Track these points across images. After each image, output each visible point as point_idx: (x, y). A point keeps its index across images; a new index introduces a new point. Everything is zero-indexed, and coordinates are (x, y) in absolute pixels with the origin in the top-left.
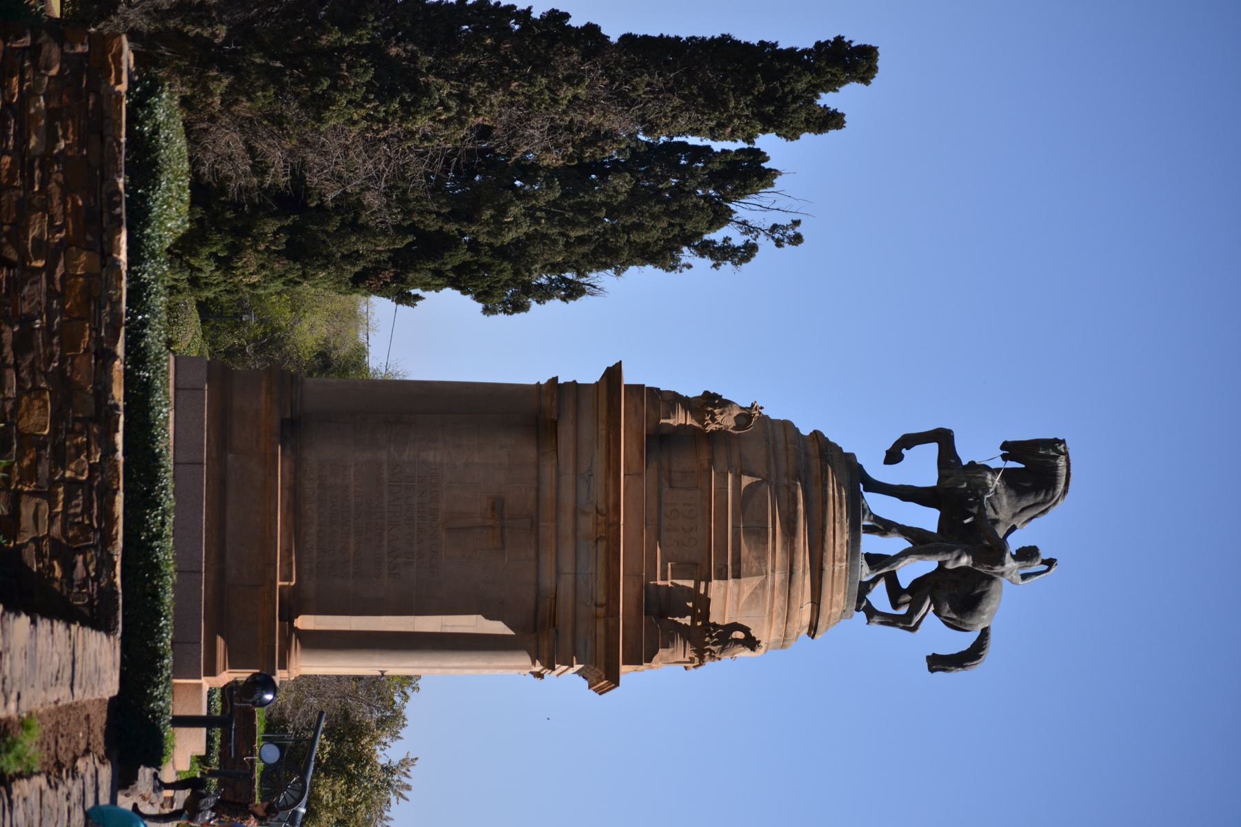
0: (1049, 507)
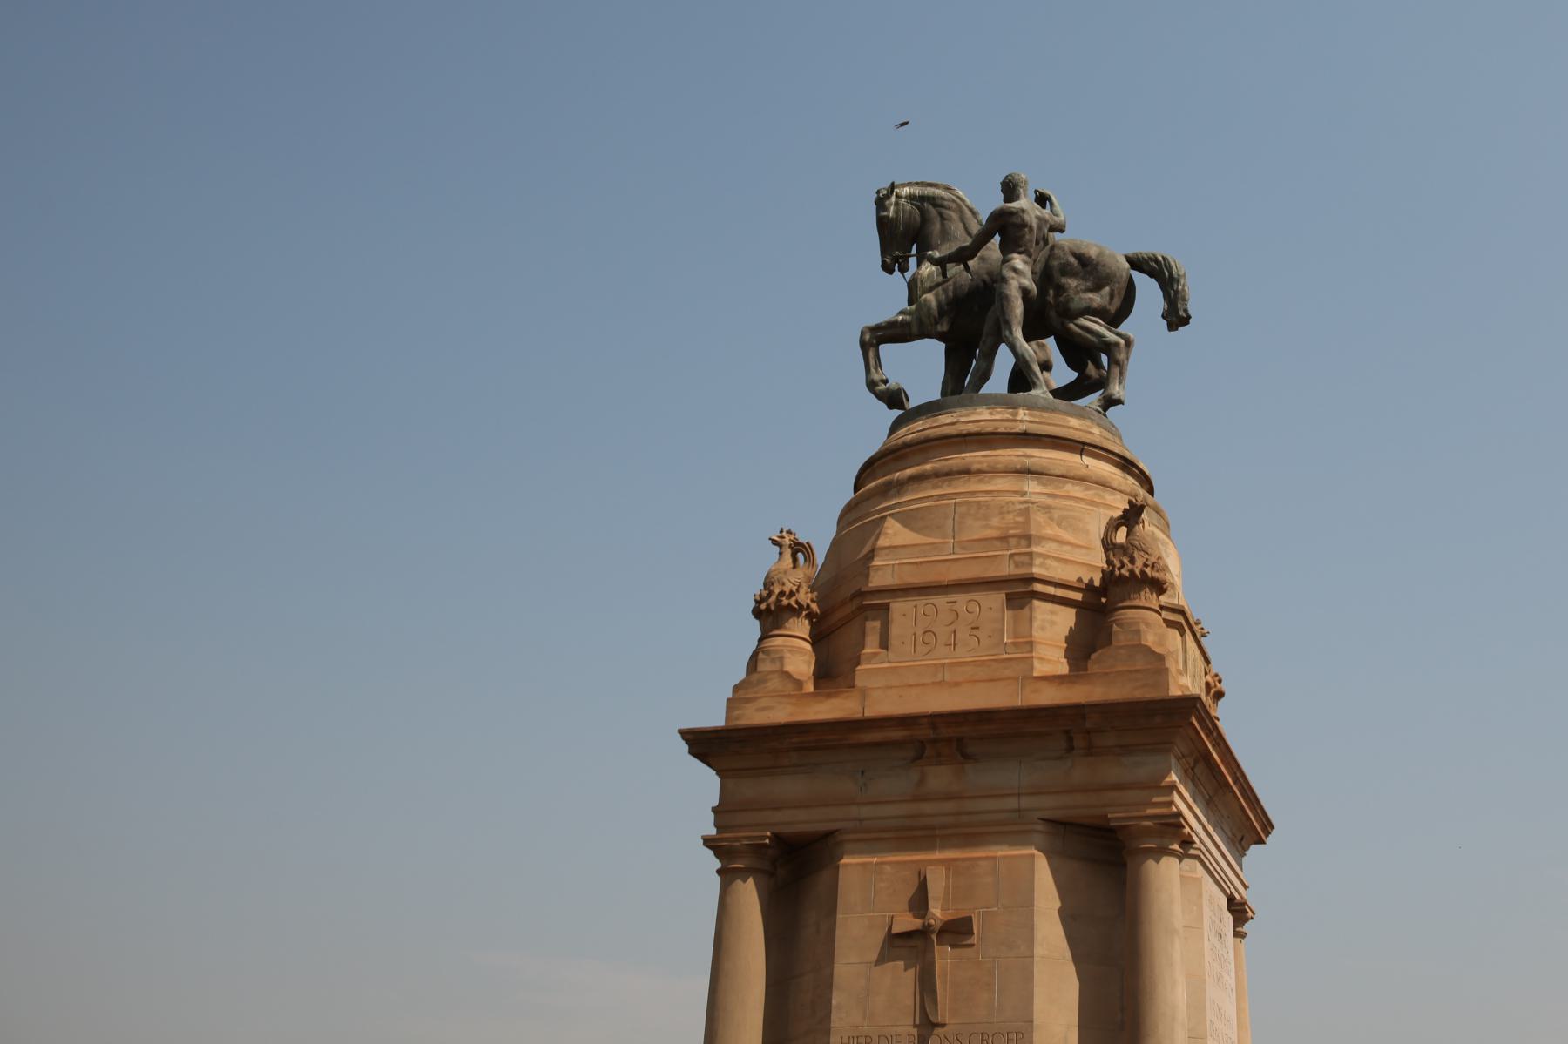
0: (967, 207)
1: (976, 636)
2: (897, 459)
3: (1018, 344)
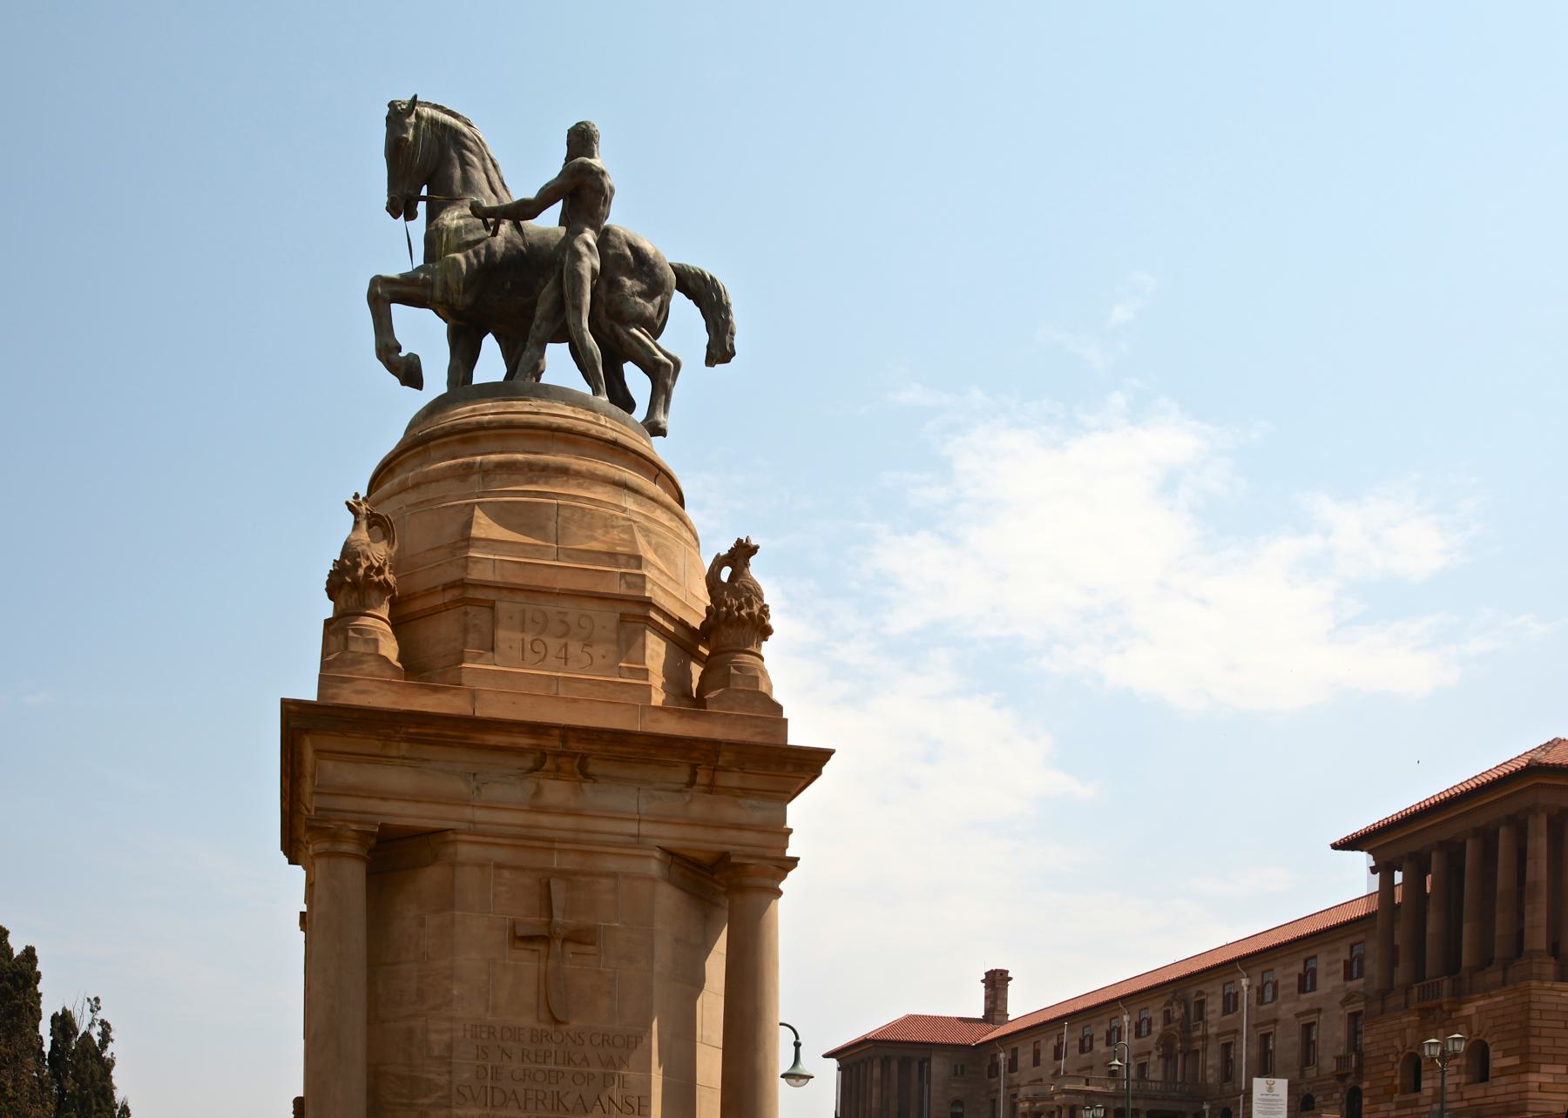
0: (488, 155)
1: (589, 654)
2: (464, 441)
3: (582, 339)
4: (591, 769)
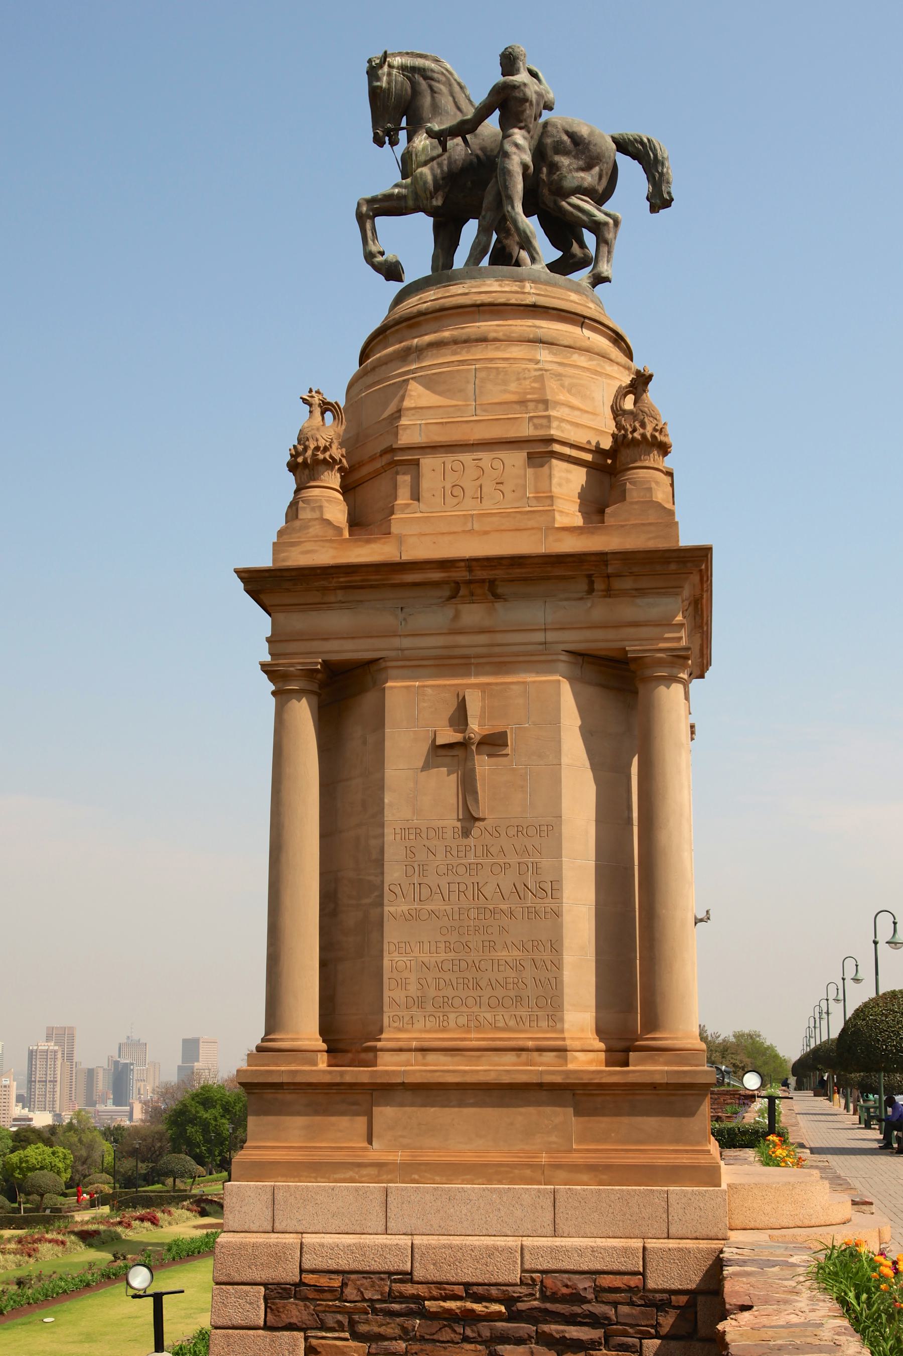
0: (455, 80)
2: (410, 327)
4: (500, 591)
